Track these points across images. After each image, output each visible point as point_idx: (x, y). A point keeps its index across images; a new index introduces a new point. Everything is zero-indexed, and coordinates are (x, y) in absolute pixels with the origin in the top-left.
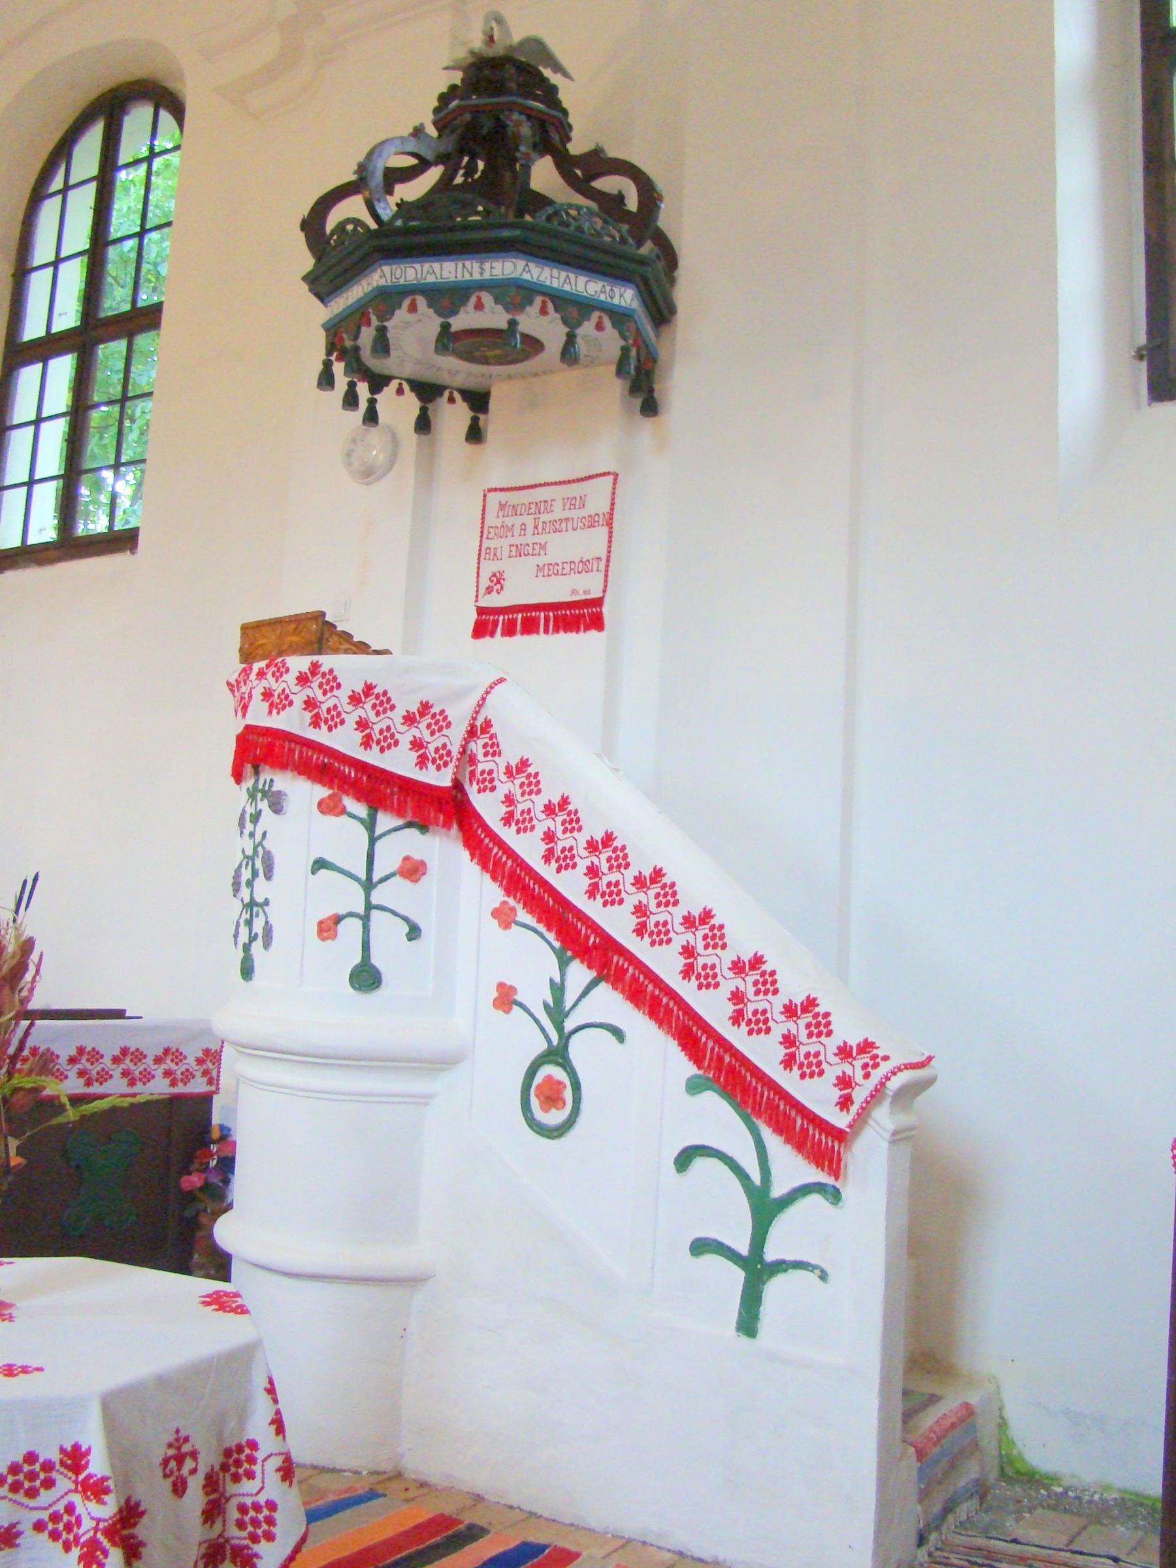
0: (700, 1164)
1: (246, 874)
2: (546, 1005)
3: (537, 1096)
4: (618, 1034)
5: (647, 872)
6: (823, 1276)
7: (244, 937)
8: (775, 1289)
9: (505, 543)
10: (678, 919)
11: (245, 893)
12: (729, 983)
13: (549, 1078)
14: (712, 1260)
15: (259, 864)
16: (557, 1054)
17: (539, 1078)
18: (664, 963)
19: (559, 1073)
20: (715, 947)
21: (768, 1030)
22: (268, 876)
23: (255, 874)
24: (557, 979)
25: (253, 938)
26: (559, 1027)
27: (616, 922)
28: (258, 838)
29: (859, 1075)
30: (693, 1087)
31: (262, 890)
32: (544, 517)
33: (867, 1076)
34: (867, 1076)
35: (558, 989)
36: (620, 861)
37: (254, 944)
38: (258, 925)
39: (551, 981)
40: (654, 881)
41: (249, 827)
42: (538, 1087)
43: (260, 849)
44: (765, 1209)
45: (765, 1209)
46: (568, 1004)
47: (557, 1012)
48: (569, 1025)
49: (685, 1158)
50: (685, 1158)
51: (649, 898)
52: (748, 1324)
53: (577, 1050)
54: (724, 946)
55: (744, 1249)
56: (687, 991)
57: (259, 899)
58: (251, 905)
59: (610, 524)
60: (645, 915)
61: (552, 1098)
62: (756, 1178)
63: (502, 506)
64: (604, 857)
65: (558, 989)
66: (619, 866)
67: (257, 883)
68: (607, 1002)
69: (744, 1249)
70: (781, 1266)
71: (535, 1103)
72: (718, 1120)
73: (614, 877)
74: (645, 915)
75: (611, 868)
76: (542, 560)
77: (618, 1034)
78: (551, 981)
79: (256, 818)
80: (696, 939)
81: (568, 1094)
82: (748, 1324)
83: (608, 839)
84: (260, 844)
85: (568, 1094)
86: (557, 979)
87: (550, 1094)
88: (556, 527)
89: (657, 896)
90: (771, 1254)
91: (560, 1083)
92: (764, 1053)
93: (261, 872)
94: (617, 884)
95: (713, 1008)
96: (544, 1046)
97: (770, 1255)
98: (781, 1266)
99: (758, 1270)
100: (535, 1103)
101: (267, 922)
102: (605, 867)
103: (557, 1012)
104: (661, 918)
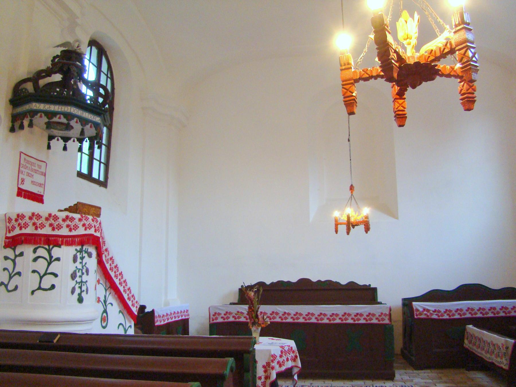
1: (79, 274)
7: (78, 291)
9: (26, 171)
11: (78, 279)
15: (84, 271)
22: (88, 274)
23: (83, 274)
25: (82, 292)
28: (84, 264)
31: (85, 278)
32: (33, 167)
37: (83, 293)
38: (84, 288)
41: (79, 260)
43: (84, 267)
57: (84, 280)
58: (82, 282)
59: (45, 175)
63: (25, 159)
67: (83, 276)
76: (33, 180)
79: (82, 258)
84: (85, 265)
88: (36, 171)
93: (85, 273)
101: (87, 287)
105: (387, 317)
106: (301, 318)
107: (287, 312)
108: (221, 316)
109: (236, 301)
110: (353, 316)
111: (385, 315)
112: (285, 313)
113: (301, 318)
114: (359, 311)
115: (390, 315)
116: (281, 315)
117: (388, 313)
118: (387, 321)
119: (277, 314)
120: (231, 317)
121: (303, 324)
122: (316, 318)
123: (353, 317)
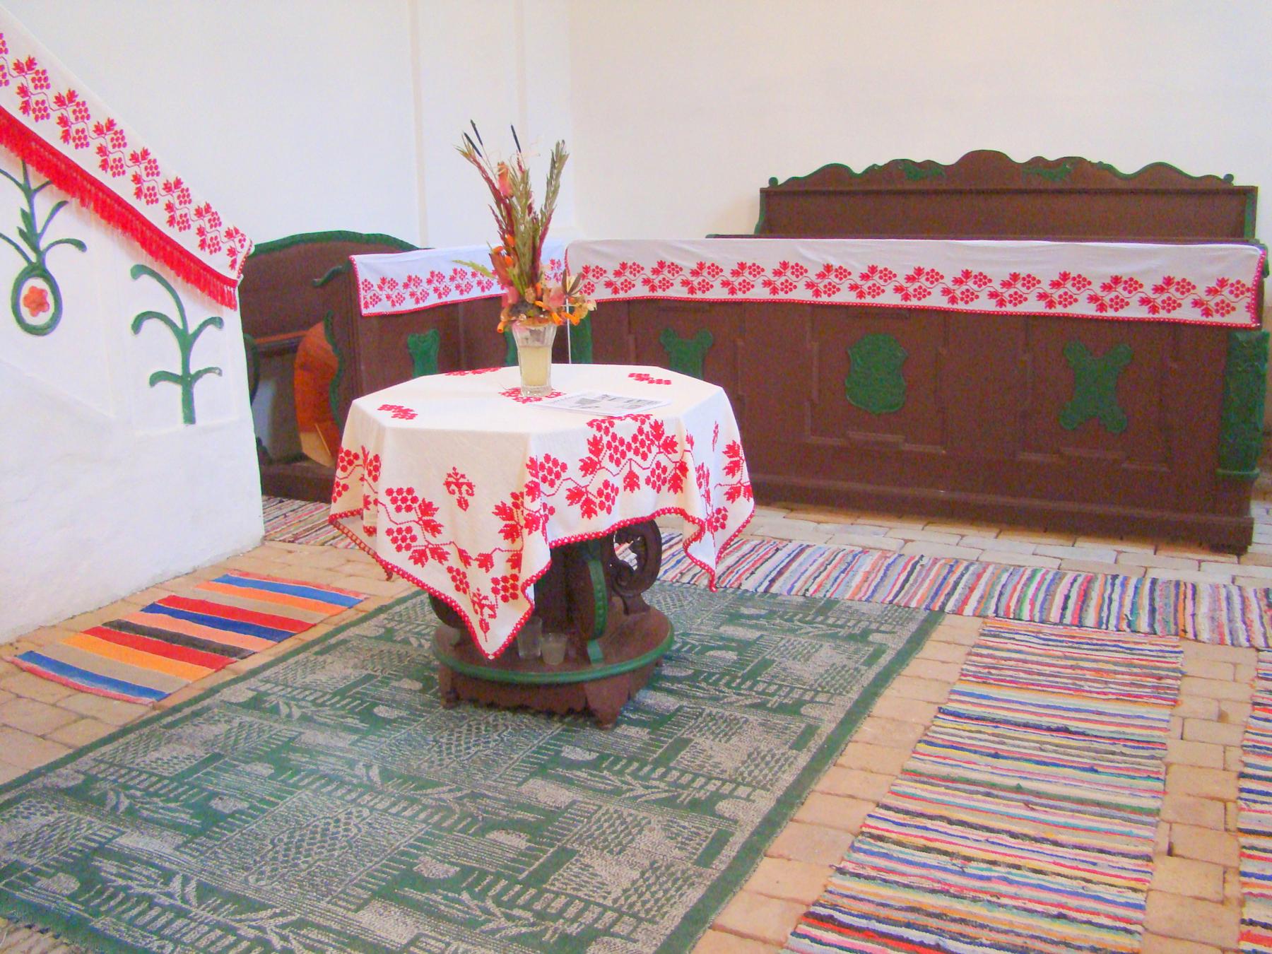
0: (149, 325)
2: (21, 231)
3: (27, 305)
4: (81, 246)
5: (103, 122)
6: (220, 374)
8: (199, 388)
10: (128, 157)
12: (164, 199)
13: (33, 289)
14: (164, 386)
16: (38, 269)
17: (25, 291)
18: (122, 187)
19: (40, 283)
20: (153, 174)
21: (189, 227)
24: (27, 209)
26: (35, 248)
27: (87, 160)
29: (238, 245)
30: (138, 271)
33: (242, 246)
34: (242, 246)
35: (28, 217)
36: (83, 112)
39: (23, 212)
40: (109, 129)
42: (26, 298)
44: (186, 341)
45: (186, 341)
46: (39, 230)
47: (31, 235)
48: (43, 245)
49: (137, 326)
50: (137, 326)
51: (106, 141)
52: (190, 418)
53: (51, 265)
54: (158, 174)
55: (179, 372)
56: (140, 206)
60: (105, 154)
61: (38, 303)
62: (180, 325)
64: (70, 109)
65: (28, 217)
66: (83, 118)
68: (70, 222)
69: (179, 372)
70: (199, 374)
71: (25, 312)
72: (152, 294)
73: (80, 126)
74: (105, 154)
75: (77, 119)
77: (81, 246)
78: (23, 212)
80: (140, 169)
81: (50, 299)
82: (190, 418)
83: (72, 95)
85: (50, 299)
86: (27, 209)
87: (38, 300)
89: (112, 140)
90: (193, 371)
91: (42, 291)
92: (188, 241)
94: (83, 131)
95: (156, 215)
96: (25, 264)
97: (193, 371)
98: (199, 374)
99: (187, 380)
100: (25, 312)
102: (72, 118)
103: (31, 235)
104: (117, 156)
105: (1246, 299)
106: (889, 288)
107: (836, 264)
108: (603, 279)
109: (752, 232)
110: (1096, 289)
111: (1238, 289)
112: (828, 268)
113: (889, 288)
114: (1124, 271)
115: (1259, 290)
116: (812, 276)
117: (1249, 281)
118: (1240, 316)
119: (799, 270)
120: (638, 282)
121: (894, 312)
122: (946, 292)
123: (1048, 290)
